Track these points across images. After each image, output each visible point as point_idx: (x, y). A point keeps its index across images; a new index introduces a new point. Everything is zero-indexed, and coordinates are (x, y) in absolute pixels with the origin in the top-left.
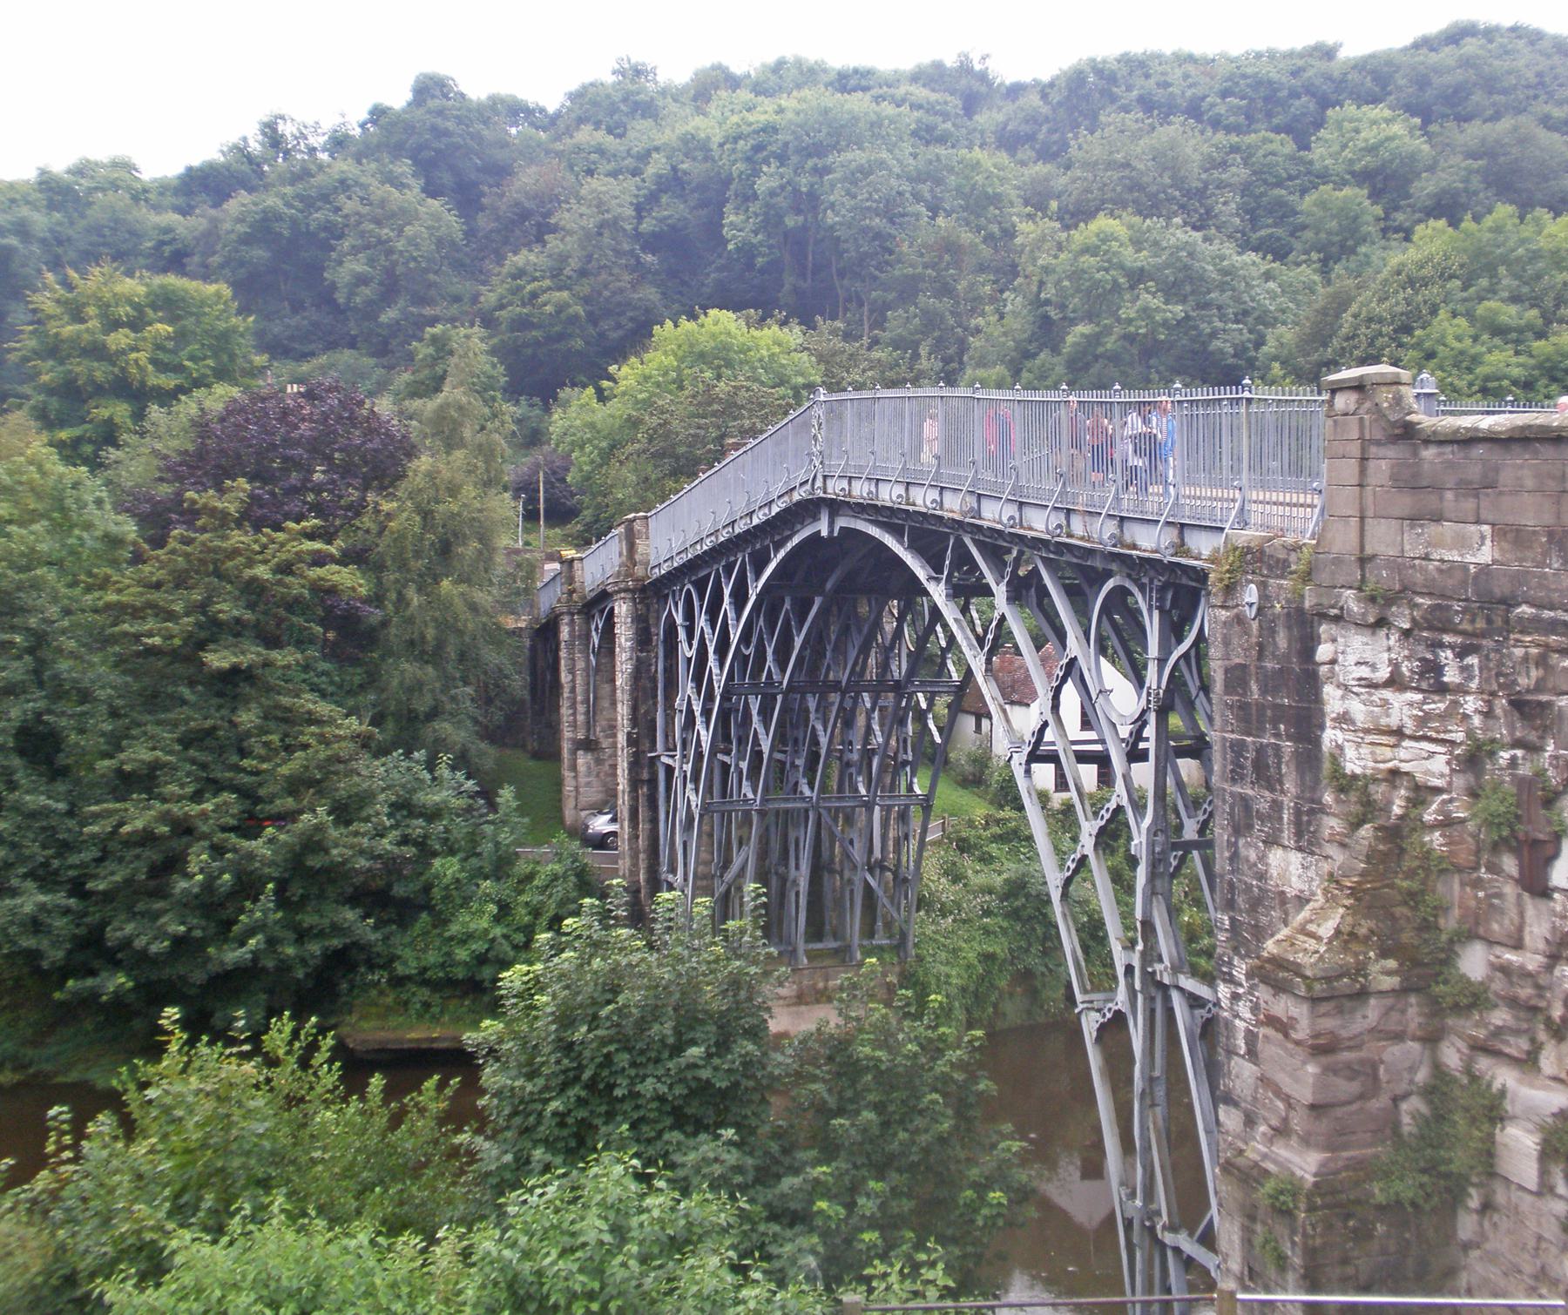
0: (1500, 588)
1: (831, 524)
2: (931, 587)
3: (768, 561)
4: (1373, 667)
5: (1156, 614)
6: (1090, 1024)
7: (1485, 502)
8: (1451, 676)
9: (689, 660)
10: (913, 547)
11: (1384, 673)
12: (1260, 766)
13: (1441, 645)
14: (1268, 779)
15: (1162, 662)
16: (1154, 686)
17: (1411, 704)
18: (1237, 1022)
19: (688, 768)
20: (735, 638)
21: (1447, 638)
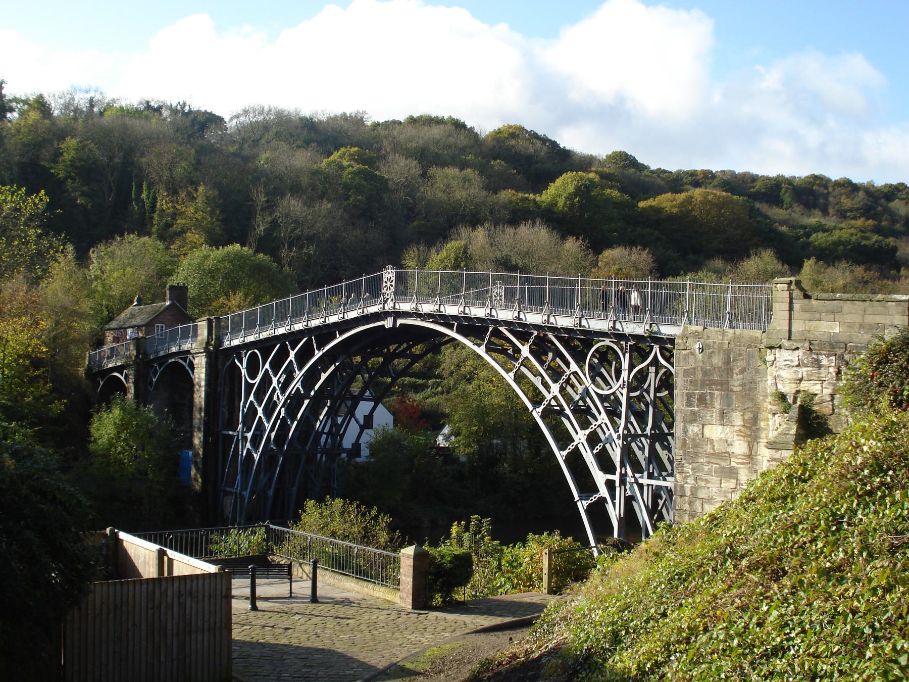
0: (843, 338)
1: (395, 322)
2: (475, 348)
3: (335, 337)
4: (792, 361)
5: (627, 355)
6: (582, 506)
7: (836, 316)
8: (825, 362)
9: (249, 387)
10: (458, 332)
11: (796, 363)
12: (702, 400)
13: (821, 354)
14: (706, 404)
15: (630, 371)
16: (626, 379)
17: (808, 371)
18: (686, 485)
19: (249, 435)
20: (299, 375)
21: (822, 352)
